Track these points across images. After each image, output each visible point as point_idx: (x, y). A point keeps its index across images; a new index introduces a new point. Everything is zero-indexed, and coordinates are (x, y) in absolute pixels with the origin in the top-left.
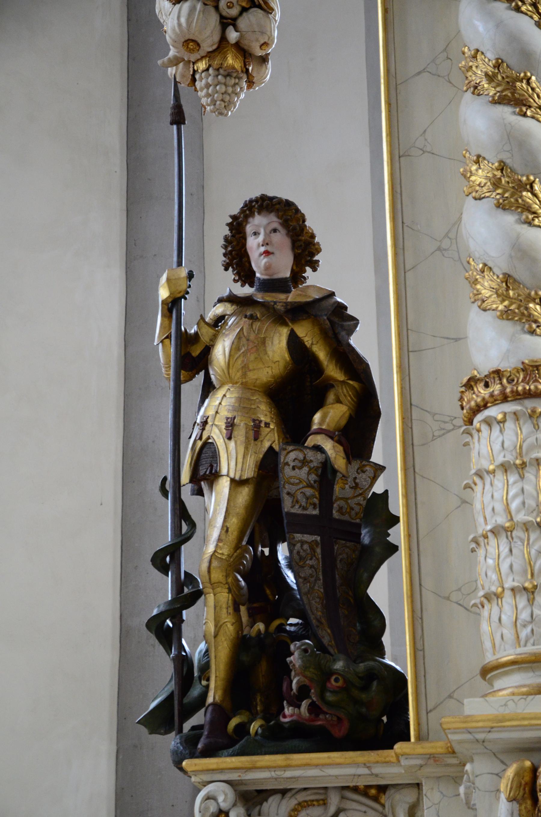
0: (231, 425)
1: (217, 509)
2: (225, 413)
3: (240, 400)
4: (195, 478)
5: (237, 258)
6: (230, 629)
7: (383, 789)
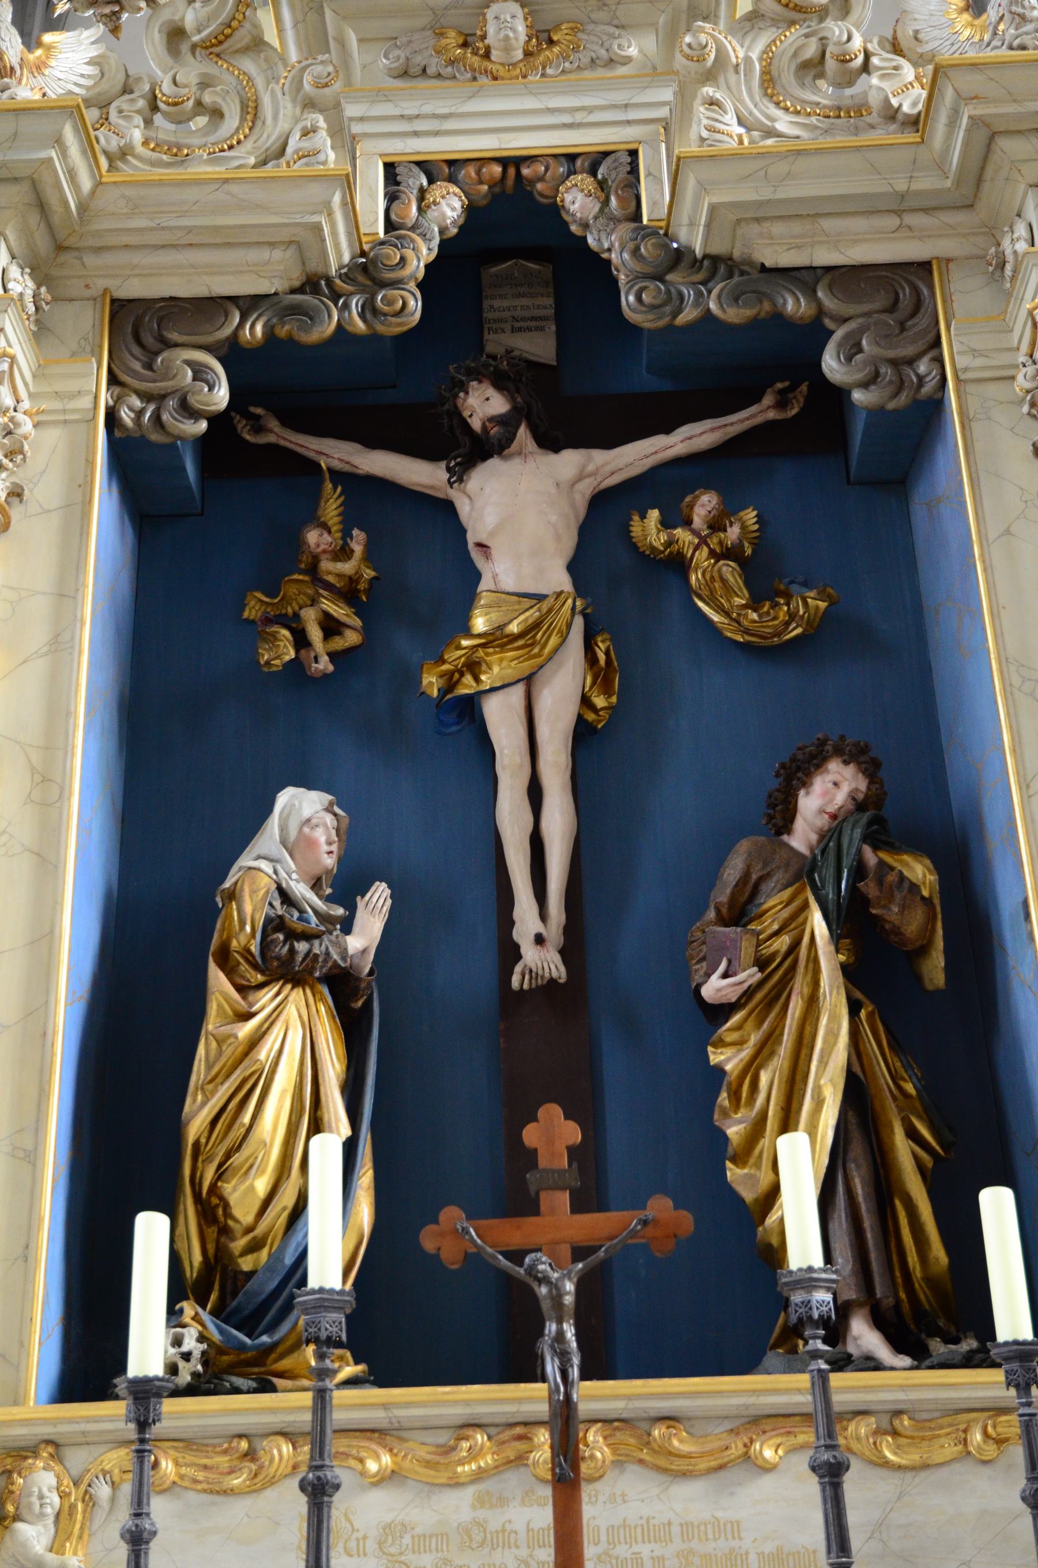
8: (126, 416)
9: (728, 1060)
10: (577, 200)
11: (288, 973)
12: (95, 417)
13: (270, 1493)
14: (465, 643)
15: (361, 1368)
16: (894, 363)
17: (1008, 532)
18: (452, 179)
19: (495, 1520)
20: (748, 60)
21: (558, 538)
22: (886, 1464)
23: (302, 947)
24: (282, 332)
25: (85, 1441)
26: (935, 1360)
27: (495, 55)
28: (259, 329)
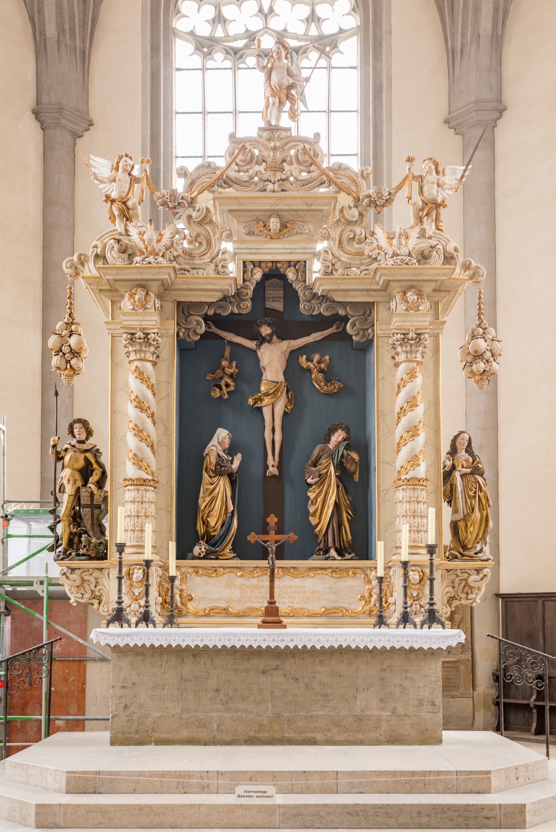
0: (69, 480)
1: (65, 499)
2: (67, 477)
3: (71, 473)
4: (60, 491)
6: (68, 531)
7: (102, 569)
8: (181, 334)
9: (312, 495)
10: (291, 275)
11: (220, 474)
12: (174, 336)
13: (219, 578)
14: (259, 395)
15: (235, 554)
16: (363, 330)
17: (383, 378)
18: (260, 266)
19: (261, 584)
20: (336, 238)
21: (281, 367)
22: (333, 577)
23: (223, 469)
24: (218, 312)
25: (184, 567)
26: (345, 558)
27: (272, 231)
28: (212, 311)
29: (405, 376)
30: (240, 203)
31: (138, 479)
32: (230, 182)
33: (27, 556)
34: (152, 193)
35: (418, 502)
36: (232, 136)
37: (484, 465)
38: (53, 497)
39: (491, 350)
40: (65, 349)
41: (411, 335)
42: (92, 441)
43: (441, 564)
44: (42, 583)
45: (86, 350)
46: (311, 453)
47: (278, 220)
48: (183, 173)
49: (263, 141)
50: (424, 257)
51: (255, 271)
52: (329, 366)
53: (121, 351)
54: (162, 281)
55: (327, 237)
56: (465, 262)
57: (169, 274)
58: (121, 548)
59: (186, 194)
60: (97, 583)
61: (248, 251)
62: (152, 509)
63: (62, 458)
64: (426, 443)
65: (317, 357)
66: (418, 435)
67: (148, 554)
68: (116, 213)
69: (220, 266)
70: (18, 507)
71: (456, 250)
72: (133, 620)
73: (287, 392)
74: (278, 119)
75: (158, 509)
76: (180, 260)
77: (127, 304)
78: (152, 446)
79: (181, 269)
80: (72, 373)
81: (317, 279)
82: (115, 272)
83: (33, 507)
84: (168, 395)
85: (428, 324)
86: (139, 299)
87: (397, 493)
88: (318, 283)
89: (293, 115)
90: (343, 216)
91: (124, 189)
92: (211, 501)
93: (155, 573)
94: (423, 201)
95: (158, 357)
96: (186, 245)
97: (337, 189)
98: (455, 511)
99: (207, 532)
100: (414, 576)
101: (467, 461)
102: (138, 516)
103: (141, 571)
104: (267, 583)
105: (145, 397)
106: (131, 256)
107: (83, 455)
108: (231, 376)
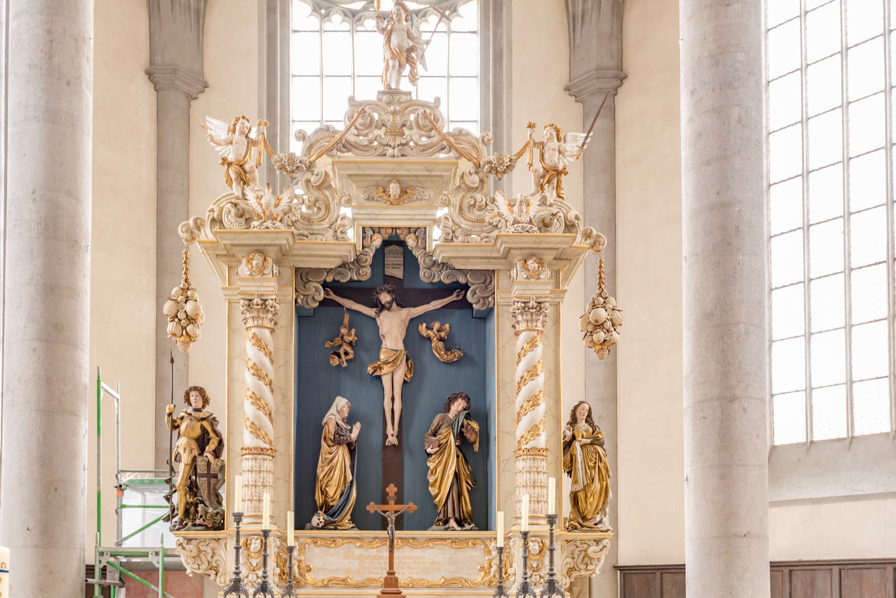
0: (185, 449)
1: (181, 468)
5: (188, 400)
6: (184, 501)
8: (299, 301)
10: (411, 242)
16: (483, 298)
18: (379, 233)
19: (380, 554)
24: (337, 279)
25: (303, 537)
29: (525, 345)
30: (359, 168)
31: (256, 448)
32: (349, 146)
33: (141, 527)
34: (269, 156)
35: (538, 473)
36: (351, 99)
37: (604, 435)
38: (168, 466)
39: (611, 320)
40: (181, 315)
41: (532, 303)
42: (208, 409)
43: (560, 535)
44: (157, 554)
45: (202, 317)
46: (431, 422)
47: (398, 185)
48: (301, 136)
49: (383, 105)
50: (545, 225)
51: (374, 237)
52: (449, 335)
53: (239, 318)
54: (280, 246)
55: (448, 204)
56: (586, 230)
57: (287, 240)
58: (238, 518)
59: (305, 158)
60: (214, 553)
61: (367, 217)
62: (270, 478)
63: (178, 426)
64: (546, 413)
65: (437, 326)
66: (539, 405)
67: (266, 524)
68: (233, 176)
69: (339, 231)
70: (132, 477)
71: (577, 218)
72: (251, 591)
73: (407, 361)
74: (398, 82)
75: (276, 479)
76: (298, 225)
77: (244, 270)
78: (270, 414)
79: (299, 235)
80: (188, 339)
81: (437, 246)
82: (232, 236)
83: (147, 477)
84: (286, 363)
85: (548, 292)
86: (257, 264)
87: (518, 463)
88: (438, 250)
89: (413, 79)
90: (464, 183)
91: (240, 152)
92: (330, 471)
93: (273, 544)
94: (544, 168)
95: (276, 324)
96: (304, 209)
97: (457, 155)
98: (575, 482)
99: (325, 502)
100: (534, 547)
101: (587, 431)
102: (255, 486)
103: (259, 541)
104: (386, 554)
105: (262, 364)
106: (248, 221)
107: (199, 424)
108: (350, 344)
